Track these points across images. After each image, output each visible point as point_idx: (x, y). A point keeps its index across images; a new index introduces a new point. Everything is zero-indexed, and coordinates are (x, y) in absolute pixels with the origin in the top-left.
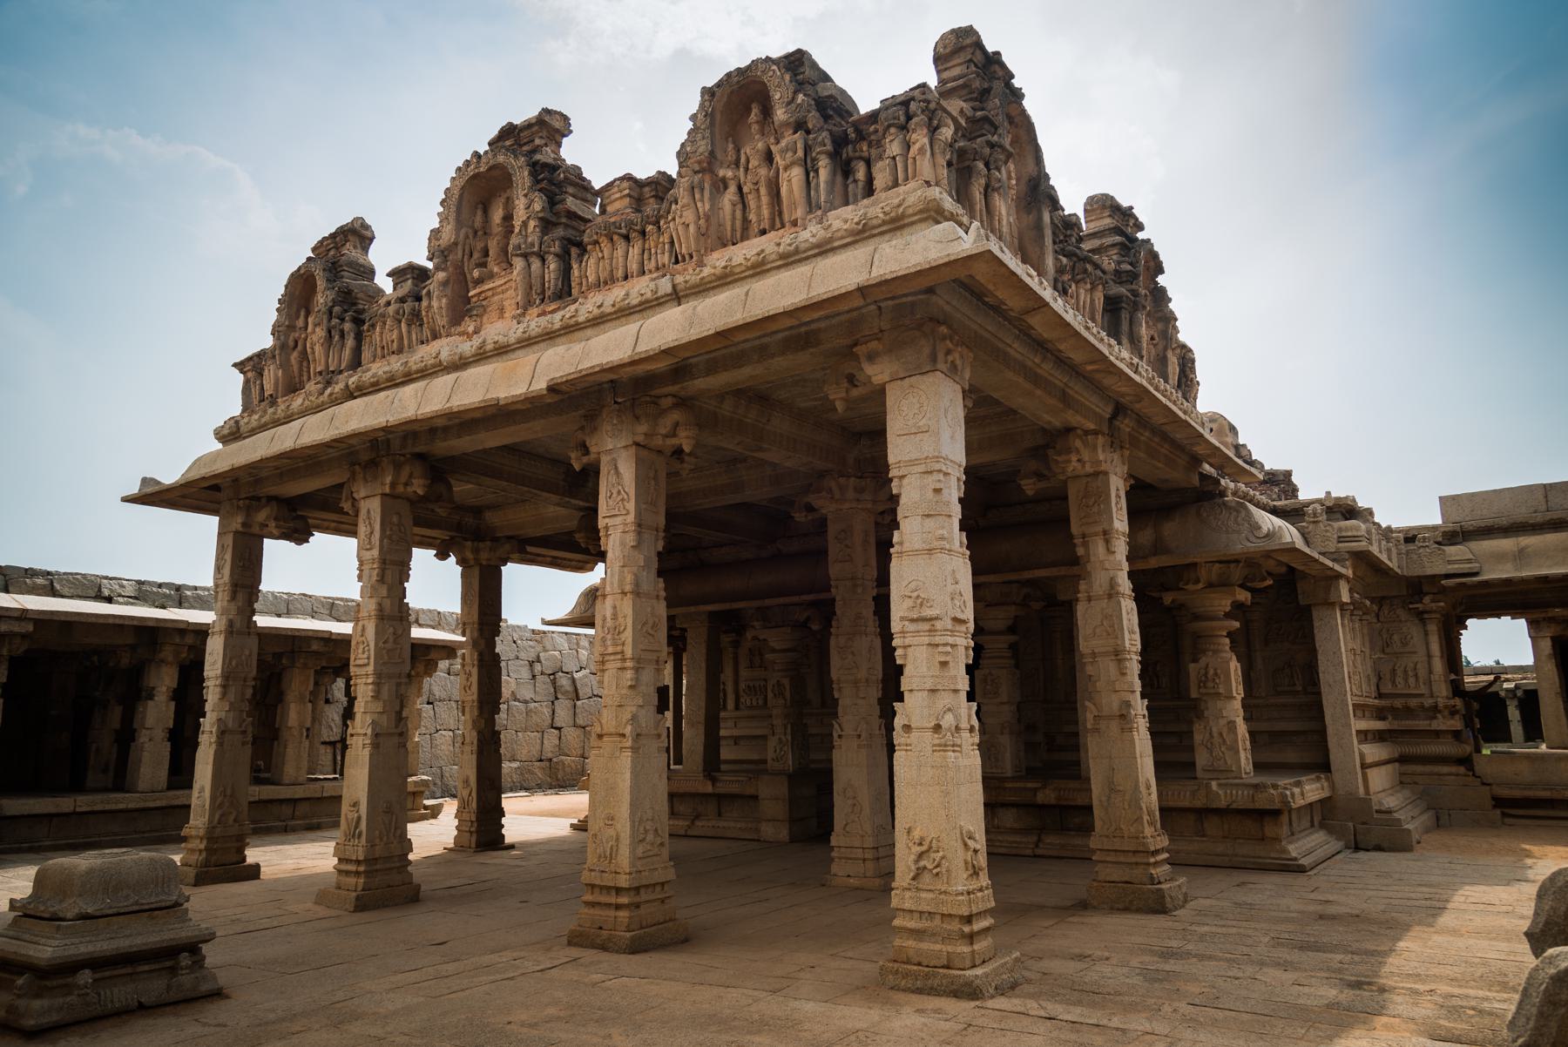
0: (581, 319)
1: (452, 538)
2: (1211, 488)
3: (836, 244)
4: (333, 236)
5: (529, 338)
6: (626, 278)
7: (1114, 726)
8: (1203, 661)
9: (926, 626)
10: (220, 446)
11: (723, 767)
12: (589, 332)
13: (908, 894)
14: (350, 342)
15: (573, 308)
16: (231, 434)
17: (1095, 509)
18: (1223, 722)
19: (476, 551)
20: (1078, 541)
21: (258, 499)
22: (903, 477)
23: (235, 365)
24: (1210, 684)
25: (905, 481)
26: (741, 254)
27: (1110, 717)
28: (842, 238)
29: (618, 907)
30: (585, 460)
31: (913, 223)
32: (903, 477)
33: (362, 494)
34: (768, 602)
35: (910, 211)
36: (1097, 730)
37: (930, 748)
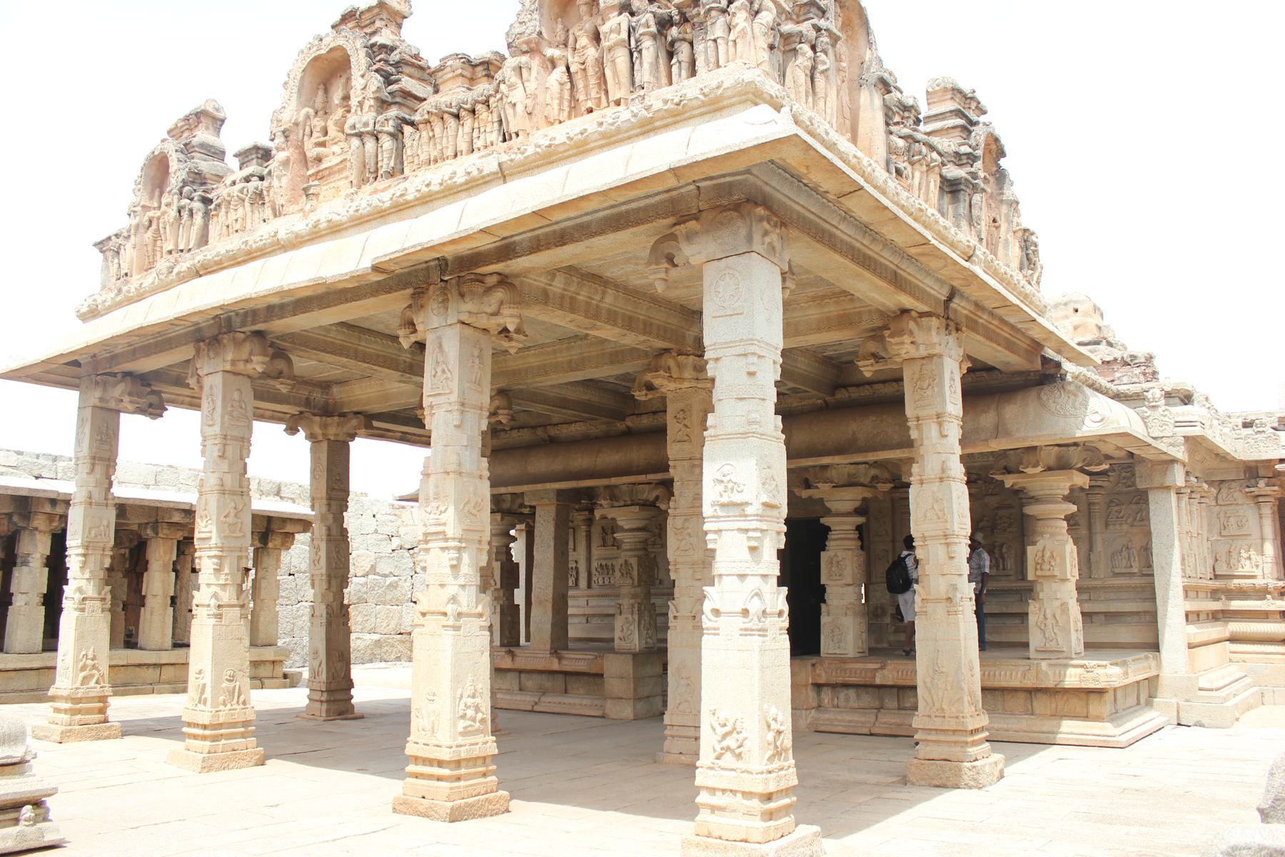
0: (410, 197)
1: (301, 413)
2: (1052, 371)
3: (658, 124)
5: (362, 217)
7: (941, 610)
9: (737, 511)
11: (570, 644)
12: (418, 210)
14: (198, 218)
15: (402, 186)
17: (929, 392)
18: (1057, 603)
19: (324, 426)
21: (114, 375)
23: (95, 245)
24: (1046, 567)
25: (720, 363)
27: (937, 601)
28: (662, 119)
31: (733, 105)
32: (717, 360)
33: (206, 372)
34: (614, 481)
35: (729, 93)
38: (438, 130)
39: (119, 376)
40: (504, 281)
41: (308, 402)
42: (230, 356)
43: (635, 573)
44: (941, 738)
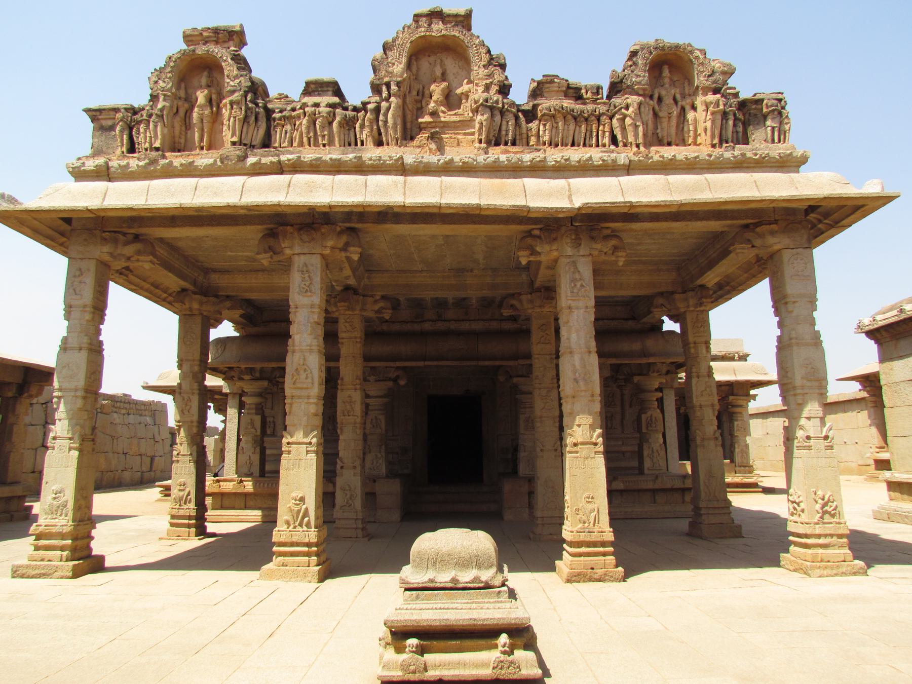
1: (184, 290)
3: (745, 165)
8: (649, 414)
12: (550, 174)
13: (817, 526)
17: (702, 329)
19: (201, 303)
20: (692, 345)
21: (125, 234)
22: (794, 302)
23: (87, 111)
25: (796, 305)
29: (604, 554)
30: (532, 259)
32: (794, 302)
33: (297, 250)
36: (703, 446)
37: (823, 448)
39: (130, 237)
40: (614, 235)
41: (195, 283)
42: (330, 243)
43: (383, 426)
44: (717, 511)
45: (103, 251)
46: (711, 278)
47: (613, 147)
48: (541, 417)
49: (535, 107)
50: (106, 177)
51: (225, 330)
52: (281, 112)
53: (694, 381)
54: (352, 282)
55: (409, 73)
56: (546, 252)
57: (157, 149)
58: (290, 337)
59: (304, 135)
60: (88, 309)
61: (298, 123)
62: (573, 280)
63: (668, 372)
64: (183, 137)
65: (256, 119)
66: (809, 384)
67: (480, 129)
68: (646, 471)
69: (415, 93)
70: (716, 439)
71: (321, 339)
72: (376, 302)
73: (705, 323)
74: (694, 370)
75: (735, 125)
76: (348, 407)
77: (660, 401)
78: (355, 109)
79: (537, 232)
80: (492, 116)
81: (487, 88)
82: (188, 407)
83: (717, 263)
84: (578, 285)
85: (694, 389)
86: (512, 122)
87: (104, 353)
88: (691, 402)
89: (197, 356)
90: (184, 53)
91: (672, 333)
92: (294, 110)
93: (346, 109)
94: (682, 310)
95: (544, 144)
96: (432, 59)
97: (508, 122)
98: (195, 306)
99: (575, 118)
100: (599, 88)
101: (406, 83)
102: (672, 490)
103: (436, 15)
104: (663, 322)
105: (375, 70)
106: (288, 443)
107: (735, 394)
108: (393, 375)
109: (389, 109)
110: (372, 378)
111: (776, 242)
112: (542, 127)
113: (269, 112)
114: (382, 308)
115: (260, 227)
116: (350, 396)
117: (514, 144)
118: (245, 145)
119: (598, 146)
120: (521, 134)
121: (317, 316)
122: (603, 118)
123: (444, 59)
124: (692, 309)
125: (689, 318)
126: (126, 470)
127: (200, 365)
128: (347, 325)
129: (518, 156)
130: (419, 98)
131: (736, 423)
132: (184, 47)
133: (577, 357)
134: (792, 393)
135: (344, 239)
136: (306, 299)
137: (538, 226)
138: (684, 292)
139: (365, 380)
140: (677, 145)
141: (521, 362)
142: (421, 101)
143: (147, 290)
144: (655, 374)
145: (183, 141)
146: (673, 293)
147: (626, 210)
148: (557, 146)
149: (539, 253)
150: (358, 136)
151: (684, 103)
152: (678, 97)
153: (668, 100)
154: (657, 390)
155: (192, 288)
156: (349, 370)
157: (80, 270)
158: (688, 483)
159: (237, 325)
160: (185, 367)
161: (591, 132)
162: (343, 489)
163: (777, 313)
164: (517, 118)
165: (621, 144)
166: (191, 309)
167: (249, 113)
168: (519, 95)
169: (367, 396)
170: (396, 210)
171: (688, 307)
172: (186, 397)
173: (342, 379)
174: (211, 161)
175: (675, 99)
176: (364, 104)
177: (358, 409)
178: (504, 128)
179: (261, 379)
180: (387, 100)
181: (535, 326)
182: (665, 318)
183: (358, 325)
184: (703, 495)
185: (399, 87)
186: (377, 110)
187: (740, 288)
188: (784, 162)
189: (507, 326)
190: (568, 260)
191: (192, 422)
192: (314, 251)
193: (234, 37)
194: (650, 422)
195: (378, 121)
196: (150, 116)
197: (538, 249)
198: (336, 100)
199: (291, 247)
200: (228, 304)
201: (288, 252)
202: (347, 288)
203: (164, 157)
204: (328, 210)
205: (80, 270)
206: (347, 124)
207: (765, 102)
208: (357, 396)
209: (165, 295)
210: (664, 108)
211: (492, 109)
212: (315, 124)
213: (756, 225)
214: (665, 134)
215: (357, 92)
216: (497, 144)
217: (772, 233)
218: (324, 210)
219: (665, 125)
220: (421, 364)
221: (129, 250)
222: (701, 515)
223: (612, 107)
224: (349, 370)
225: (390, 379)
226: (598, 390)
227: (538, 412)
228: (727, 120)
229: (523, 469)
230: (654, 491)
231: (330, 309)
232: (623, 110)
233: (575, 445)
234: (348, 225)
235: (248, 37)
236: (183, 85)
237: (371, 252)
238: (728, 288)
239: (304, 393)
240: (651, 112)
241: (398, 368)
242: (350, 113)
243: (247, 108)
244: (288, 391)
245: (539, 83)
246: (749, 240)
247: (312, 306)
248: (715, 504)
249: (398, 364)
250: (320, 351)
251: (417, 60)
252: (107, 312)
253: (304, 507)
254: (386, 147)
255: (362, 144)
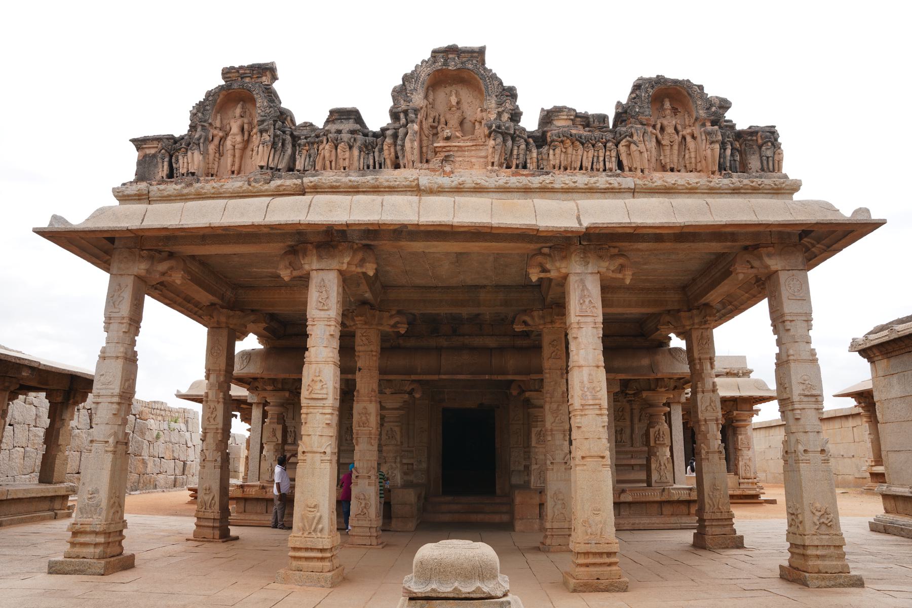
0: (556, 186)
4: (252, 68)
6: (581, 168)
8: (657, 428)
9: (813, 399)
10: (116, 203)
12: (559, 195)
16: (122, 196)
17: (707, 346)
19: (228, 317)
20: (697, 361)
21: (160, 252)
23: (134, 141)
26: (671, 178)
27: (714, 452)
30: (542, 275)
38: (570, 150)
39: (165, 254)
41: (222, 298)
42: (347, 260)
43: (398, 437)
45: (141, 268)
46: (714, 297)
47: (619, 172)
48: (552, 430)
49: (544, 134)
50: (147, 201)
51: (250, 343)
52: (306, 138)
53: (699, 396)
54: (368, 295)
55: (425, 101)
56: (556, 268)
57: (193, 174)
58: (307, 349)
59: (326, 159)
60: (124, 321)
61: (321, 148)
62: (582, 297)
63: (675, 388)
64: (216, 163)
65: (283, 145)
66: (806, 399)
67: (493, 152)
68: (653, 484)
69: (431, 120)
70: (720, 452)
71: (336, 352)
72: (392, 316)
73: (710, 340)
74: (699, 385)
75: (732, 155)
76: (364, 418)
77: (668, 416)
78: (375, 135)
79: (546, 250)
80: (505, 141)
81: (499, 114)
82: (214, 416)
83: (719, 283)
84: (587, 301)
85: (699, 404)
86: (523, 146)
87: (138, 362)
88: (697, 416)
89: (223, 366)
90: (221, 88)
91: (679, 349)
92: (317, 136)
93: (366, 135)
94: (688, 328)
95: (554, 167)
96: (448, 89)
97: (518, 147)
98: (223, 319)
99: (583, 144)
100: (604, 118)
101: (422, 111)
102: (680, 502)
103: (452, 50)
104: (670, 339)
105: (394, 98)
106: (304, 452)
107: (737, 409)
108: (408, 388)
109: (407, 134)
110: (388, 391)
111: (774, 263)
112: (551, 152)
113: (295, 138)
114: (398, 323)
115: (282, 245)
116: (365, 408)
117: (525, 167)
118: (271, 168)
119: (605, 170)
120: (531, 158)
121: (335, 330)
122: (609, 144)
123: (459, 90)
124: (696, 326)
125: (695, 335)
126: (161, 473)
127: (225, 376)
128: (364, 338)
129: (529, 178)
130: (435, 124)
131: (740, 437)
132: (223, 83)
133: (585, 371)
134: (790, 408)
135: (360, 255)
136: (322, 312)
137: (548, 245)
138: (689, 310)
139: (381, 392)
140: (679, 171)
141: (534, 377)
142: (437, 128)
143: (180, 305)
144: (663, 389)
145: (216, 166)
146: (679, 311)
147: (631, 231)
148: (566, 169)
149: (549, 271)
150: (377, 159)
151: (684, 133)
152: (679, 128)
153: (670, 130)
154: (664, 405)
155: (220, 302)
156: (366, 384)
157: (120, 285)
158: (694, 496)
159: (261, 338)
160: (212, 377)
161: (598, 157)
162: (358, 498)
163: (776, 331)
164: (527, 144)
165: (627, 169)
166: (218, 322)
167: (276, 139)
168: (530, 122)
169: (382, 408)
170: (410, 228)
171: (693, 324)
172: (212, 406)
173: (358, 391)
174: (239, 184)
175: (676, 129)
176: (383, 130)
177: (373, 420)
178: (515, 152)
179: (283, 390)
180: (405, 126)
181: (546, 340)
182: (672, 335)
183: (375, 338)
184: (707, 506)
185: (416, 115)
186: (395, 136)
187: (742, 307)
188: (778, 189)
189: (519, 342)
190: (577, 278)
191: (217, 429)
192: (332, 267)
193: (267, 71)
194: (658, 437)
195: (395, 146)
196: (189, 144)
197: (548, 266)
198: (358, 127)
199: (310, 264)
200: (252, 317)
201: (307, 267)
202: (364, 303)
203: (198, 181)
204: (345, 228)
205: (120, 285)
206: (366, 147)
207: (759, 134)
208: (373, 408)
209: (196, 309)
210: (666, 137)
211: (504, 135)
212: (336, 149)
213: (756, 247)
214: (668, 160)
215: (377, 118)
216: (508, 167)
217: (769, 255)
218: (340, 228)
219: (668, 152)
220: (436, 377)
221: (163, 267)
222: (705, 526)
223: (618, 135)
224: (366, 384)
225: (405, 392)
226: (605, 404)
227: (548, 425)
228: (725, 149)
229: (534, 481)
230: (661, 503)
231: (346, 322)
232: (628, 138)
233: (583, 458)
234: (364, 242)
235: (279, 73)
236: (219, 117)
237: (388, 268)
238: (730, 307)
239: (320, 403)
240: (654, 140)
241: (413, 381)
242: (370, 139)
243: (275, 136)
244: (304, 402)
245: (549, 112)
246: (748, 262)
247: (329, 319)
248: (719, 516)
249: (413, 377)
250: (335, 364)
251: (433, 91)
252: (142, 324)
253: (318, 514)
254: (402, 170)
255: (380, 167)
